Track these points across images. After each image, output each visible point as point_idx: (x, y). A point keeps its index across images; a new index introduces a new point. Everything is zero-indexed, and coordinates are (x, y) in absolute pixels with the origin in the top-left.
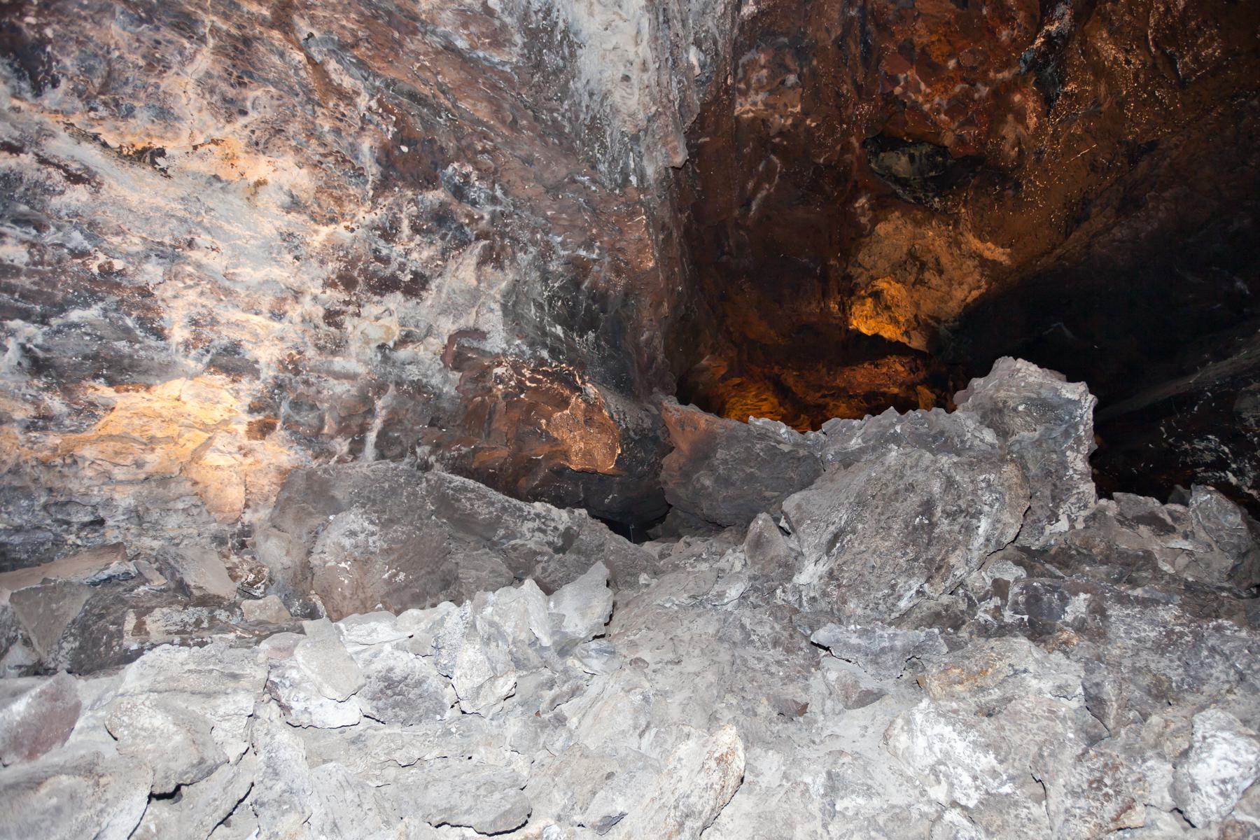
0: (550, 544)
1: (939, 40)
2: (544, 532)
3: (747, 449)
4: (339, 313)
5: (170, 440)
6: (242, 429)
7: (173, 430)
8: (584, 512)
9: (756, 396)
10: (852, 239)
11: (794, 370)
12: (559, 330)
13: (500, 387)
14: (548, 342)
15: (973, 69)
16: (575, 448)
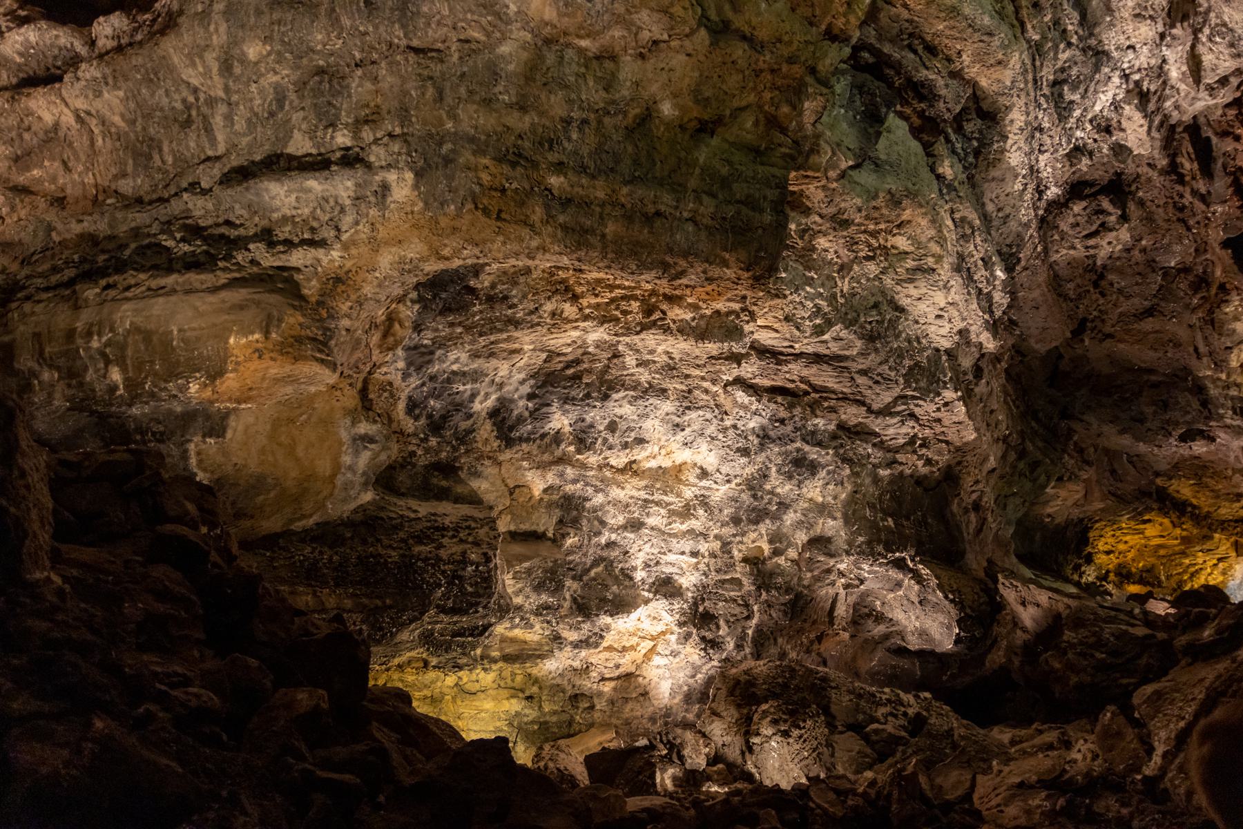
0: (903, 727)
2: (895, 716)
3: (1094, 634)
4: (729, 543)
5: (633, 648)
6: (673, 638)
7: (635, 640)
8: (928, 695)
9: (1129, 519)
10: (1227, 348)
11: (1189, 479)
12: (890, 522)
13: (843, 580)
14: (883, 537)
16: (910, 628)
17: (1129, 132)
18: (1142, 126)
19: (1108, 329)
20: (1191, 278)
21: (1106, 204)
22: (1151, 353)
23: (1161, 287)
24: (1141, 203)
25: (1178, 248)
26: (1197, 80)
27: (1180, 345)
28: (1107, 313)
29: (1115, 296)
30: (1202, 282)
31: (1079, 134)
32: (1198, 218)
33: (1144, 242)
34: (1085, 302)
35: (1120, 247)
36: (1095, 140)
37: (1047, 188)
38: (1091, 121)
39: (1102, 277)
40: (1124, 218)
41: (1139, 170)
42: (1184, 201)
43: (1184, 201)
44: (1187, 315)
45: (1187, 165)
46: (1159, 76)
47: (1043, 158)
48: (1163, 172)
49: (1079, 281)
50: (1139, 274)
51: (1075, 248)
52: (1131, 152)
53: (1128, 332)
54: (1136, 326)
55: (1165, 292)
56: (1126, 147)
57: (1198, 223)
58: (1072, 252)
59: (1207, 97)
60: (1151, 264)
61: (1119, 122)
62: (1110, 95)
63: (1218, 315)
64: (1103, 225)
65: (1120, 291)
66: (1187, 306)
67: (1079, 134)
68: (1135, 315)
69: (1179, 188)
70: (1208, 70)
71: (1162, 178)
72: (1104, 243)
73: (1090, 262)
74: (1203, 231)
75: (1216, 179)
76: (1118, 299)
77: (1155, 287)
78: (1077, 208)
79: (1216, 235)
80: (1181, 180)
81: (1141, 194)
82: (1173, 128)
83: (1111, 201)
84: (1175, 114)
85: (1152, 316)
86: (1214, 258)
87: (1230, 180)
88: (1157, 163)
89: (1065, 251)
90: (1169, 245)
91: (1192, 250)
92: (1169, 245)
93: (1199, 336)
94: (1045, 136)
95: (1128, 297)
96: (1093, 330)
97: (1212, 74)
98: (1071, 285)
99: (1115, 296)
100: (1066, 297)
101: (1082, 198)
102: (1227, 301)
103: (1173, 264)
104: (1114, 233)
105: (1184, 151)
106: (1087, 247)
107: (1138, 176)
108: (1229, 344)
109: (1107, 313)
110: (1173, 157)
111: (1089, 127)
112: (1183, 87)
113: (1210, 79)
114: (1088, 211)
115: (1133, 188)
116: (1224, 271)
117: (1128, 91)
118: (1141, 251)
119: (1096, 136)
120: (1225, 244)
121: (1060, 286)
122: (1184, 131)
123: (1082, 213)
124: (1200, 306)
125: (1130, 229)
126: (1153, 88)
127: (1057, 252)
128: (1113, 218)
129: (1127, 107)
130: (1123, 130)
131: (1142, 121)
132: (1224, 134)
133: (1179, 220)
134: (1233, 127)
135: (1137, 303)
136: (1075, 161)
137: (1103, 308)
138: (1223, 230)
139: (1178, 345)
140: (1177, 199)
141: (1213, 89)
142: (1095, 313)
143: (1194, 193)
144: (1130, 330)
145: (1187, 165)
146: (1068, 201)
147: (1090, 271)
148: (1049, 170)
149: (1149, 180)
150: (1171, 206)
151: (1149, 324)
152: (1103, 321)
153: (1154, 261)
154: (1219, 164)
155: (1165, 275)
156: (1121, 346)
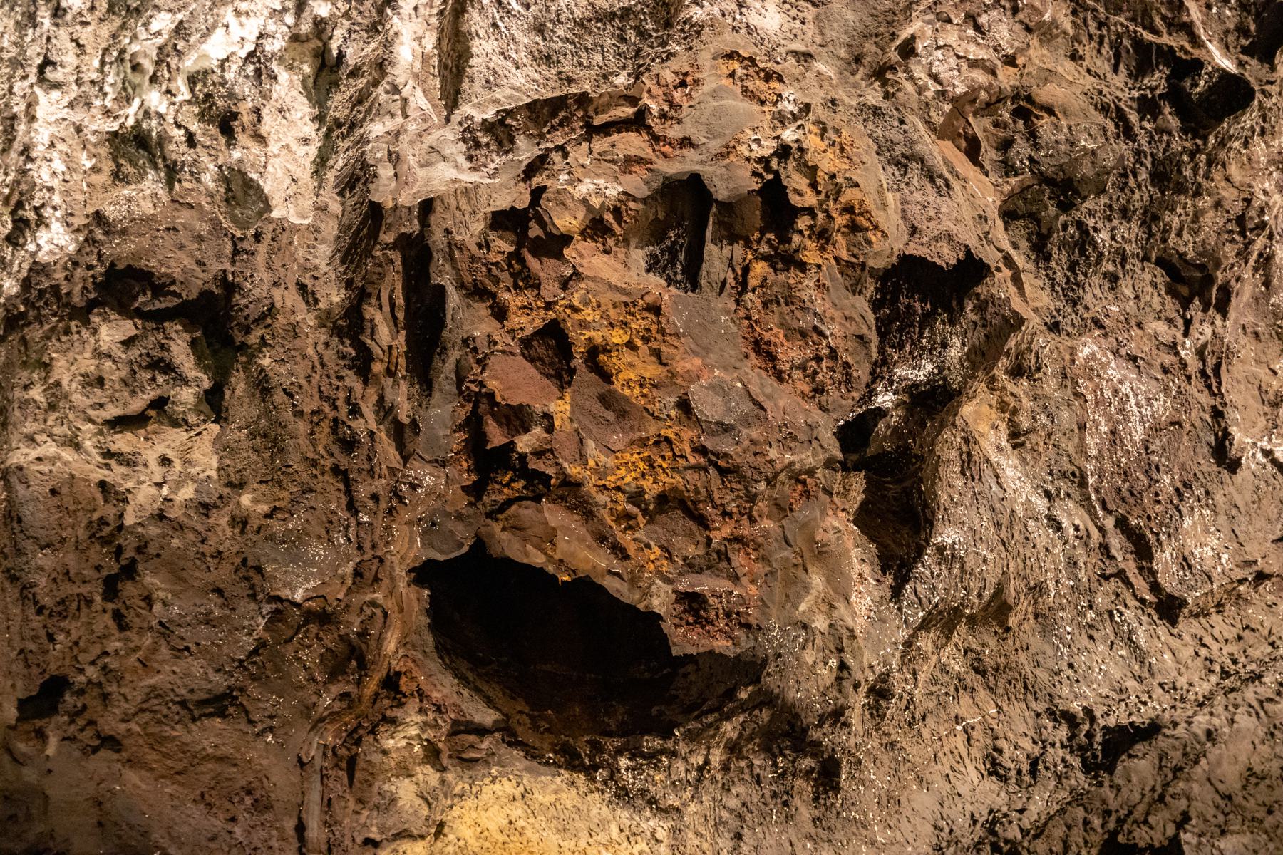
1: (630, 345)
15: (726, 429)
17: (274, 148)
18: (306, 141)
19: (111, 724)
20: (329, 639)
21: (180, 351)
22: (196, 813)
23: (262, 644)
24: (262, 386)
25: (318, 551)
26: (452, 97)
27: (269, 807)
28: (119, 680)
29: (148, 640)
30: (352, 657)
31: (155, 99)
32: (380, 485)
33: (246, 500)
34: (73, 626)
35: (187, 492)
36: (191, 140)
37: (41, 222)
38: (192, 80)
39: (129, 571)
40: (214, 403)
41: (277, 294)
42: (358, 425)
43: (358, 425)
44: (299, 733)
45: (384, 333)
46: (374, 29)
47: (50, 106)
48: (326, 320)
49: (71, 560)
50: (219, 591)
51: (77, 447)
52: (268, 208)
53: (157, 742)
54: (179, 731)
55: (263, 662)
56: (259, 190)
57: (375, 498)
58: (68, 454)
59: (461, 160)
60: (250, 571)
61: (257, 111)
62: (251, 29)
63: (368, 753)
64: (160, 403)
65: (165, 629)
66: (308, 708)
67: (155, 99)
68: (183, 704)
69: (352, 380)
70: (479, 80)
71: (323, 336)
72: (151, 456)
73: (110, 511)
74: (380, 523)
75: (437, 395)
76: (154, 650)
77: (248, 642)
78: (111, 332)
79: (406, 547)
80: (362, 363)
81: (266, 362)
82: (375, 214)
83: (193, 344)
84: (386, 172)
85: (222, 714)
86: (390, 605)
87: (463, 413)
88: (321, 292)
89: (50, 449)
90: (301, 537)
91: (349, 569)
92: (301, 537)
93: (314, 797)
94: (63, 33)
95: (180, 652)
96: (75, 715)
97: (485, 95)
98: (45, 559)
99: (148, 640)
100: (26, 593)
101: (126, 311)
102: (393, 721)
103: (299, 596)
104: (180, 435)
105: (385, 296)
106: (108, 454)
107: (271, 311)
108: (374, 834)
109: (119, 680)
110: (360, 295)
111: (184, 94)
112: (418, 100)
113: (477, 110)
114: (134, 353)
115: (253, 339)
116: (403, 643)
117: (295, 38)
118: (233, 522)
119: (195, 127)
120: (424, 574)
121: (19, 552)
122: (394, 246)
123: (118, 352)
124: (334, 716)
125: (223, 447)
126: (351, 59)
127: (31, 439)
128: (187, 396)
129: (283, 75)
130: (261, 139)
131: (309, 129)
132: (477, 292)
133: (336, 470)
134: (496, 281)
135: (199, 675)
136: (128, 168)
137: (113, 663)
138: (424, 534)
139: (262, 806)
140: (344, 410)
141: (477, 145)
142: (92, 672)
143: (385, 410)
144: (163, 740)
145: (384, 333)
146: (91, 305)
147: (106, 541)
148: (59, 166)
149: (294, 330)
150: (326, 426)
151: (211, 735)
152: (105, 697)
153: (259, 569)
154: (450, 365)
155: (276, 617)
156: (132, 776)
